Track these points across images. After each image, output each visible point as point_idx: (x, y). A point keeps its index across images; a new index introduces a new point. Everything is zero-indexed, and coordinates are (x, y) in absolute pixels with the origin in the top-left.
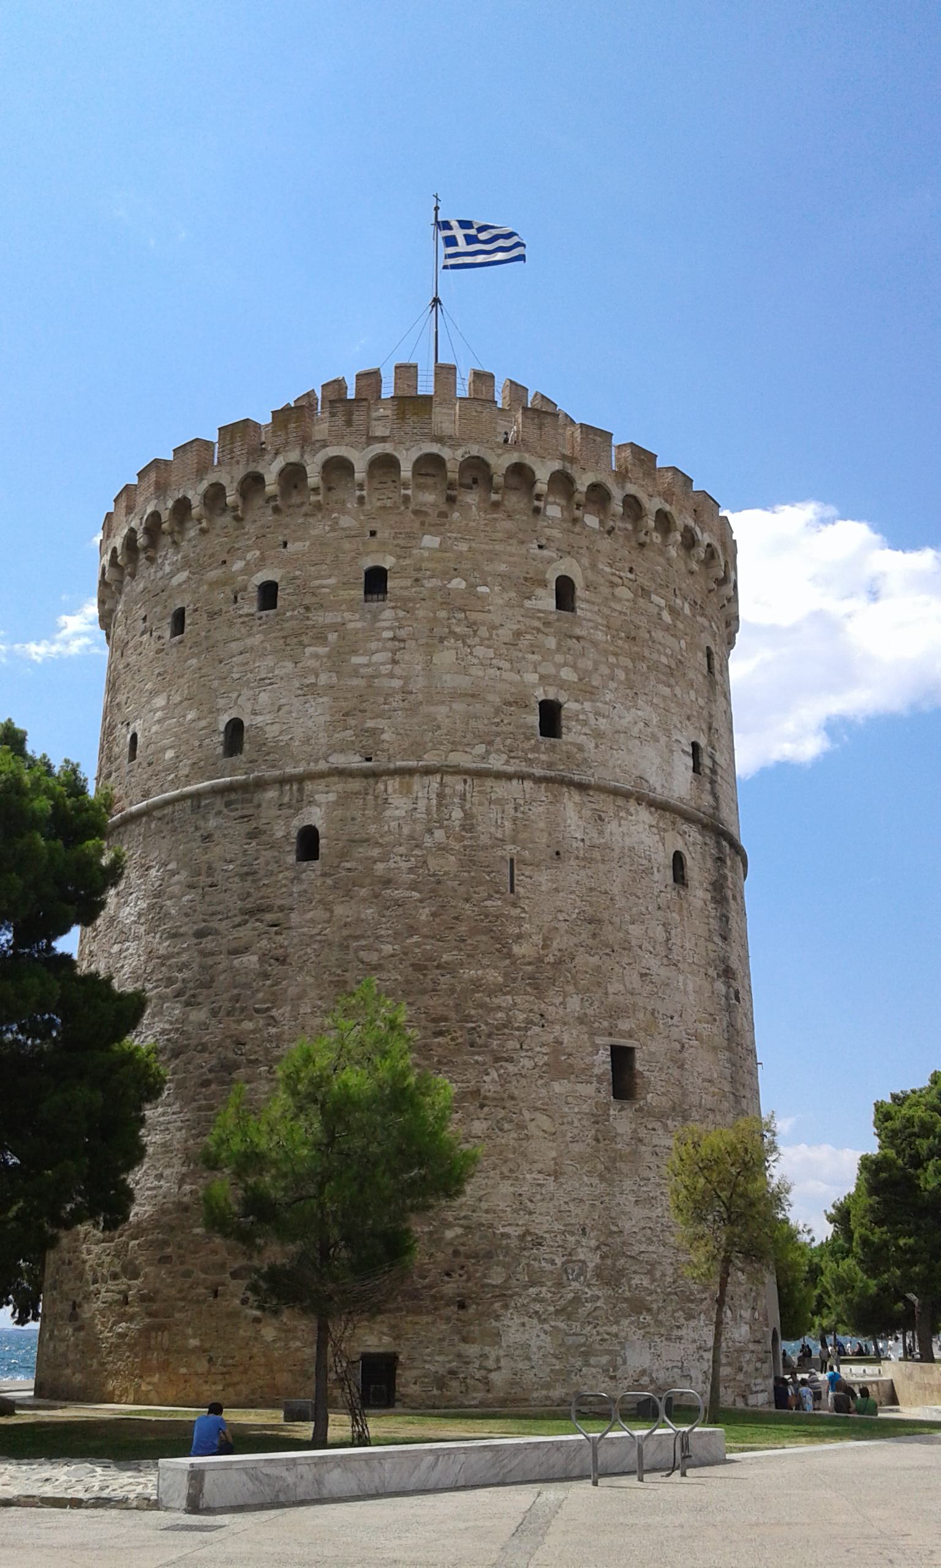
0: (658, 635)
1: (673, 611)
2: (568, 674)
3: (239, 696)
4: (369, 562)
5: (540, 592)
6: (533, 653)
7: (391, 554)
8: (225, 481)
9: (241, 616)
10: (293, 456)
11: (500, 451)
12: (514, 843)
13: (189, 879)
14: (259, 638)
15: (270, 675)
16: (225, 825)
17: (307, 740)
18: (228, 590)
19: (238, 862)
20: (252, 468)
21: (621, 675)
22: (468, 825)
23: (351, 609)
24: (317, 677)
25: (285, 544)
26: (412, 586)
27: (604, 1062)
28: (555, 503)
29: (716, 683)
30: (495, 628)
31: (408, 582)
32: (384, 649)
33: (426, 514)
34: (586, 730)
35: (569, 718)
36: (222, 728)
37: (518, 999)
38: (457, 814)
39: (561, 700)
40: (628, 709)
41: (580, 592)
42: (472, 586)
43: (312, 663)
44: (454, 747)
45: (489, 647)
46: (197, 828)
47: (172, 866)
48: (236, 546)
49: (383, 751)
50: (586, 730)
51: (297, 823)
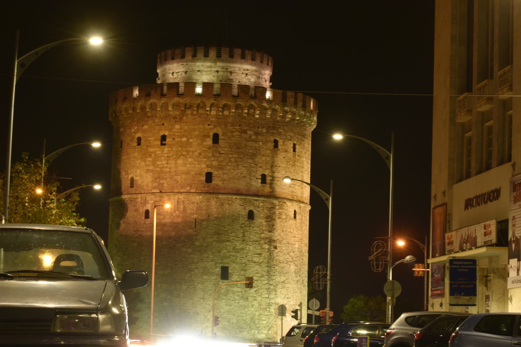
0: (250, 144)
1: (257, 134)
2: (215, 163)
4: (162, 134)
5: (208, 139)
6: (205, 158)
7: (168, 131)
11: (196, 98)
12: (196, 213)
17: (147, 186)
21: (233, 160)
22: (185, 210)
23: (157, 147)
24: (149, 166)
25: (143, 126)
26: (172, 141)
27: (219, 271)
28: (214, 110)
29: (279, 150)
30: (193, 152)
31: (171, 140)
32: (165, 160)
33: (176, 118)
34: (220, 179)
35: (214, 177)
36: (130, 179)
37: (196, 256)
38: (182, 207)
39: (212, 171)
40: (235, 171)
41: (220, 137)
42: (188, 140)
43: (148, 163)
44: (182, 187)
45: (192, 158)
49: (164, 189)
50: (220, 179)
51: (145, 208)
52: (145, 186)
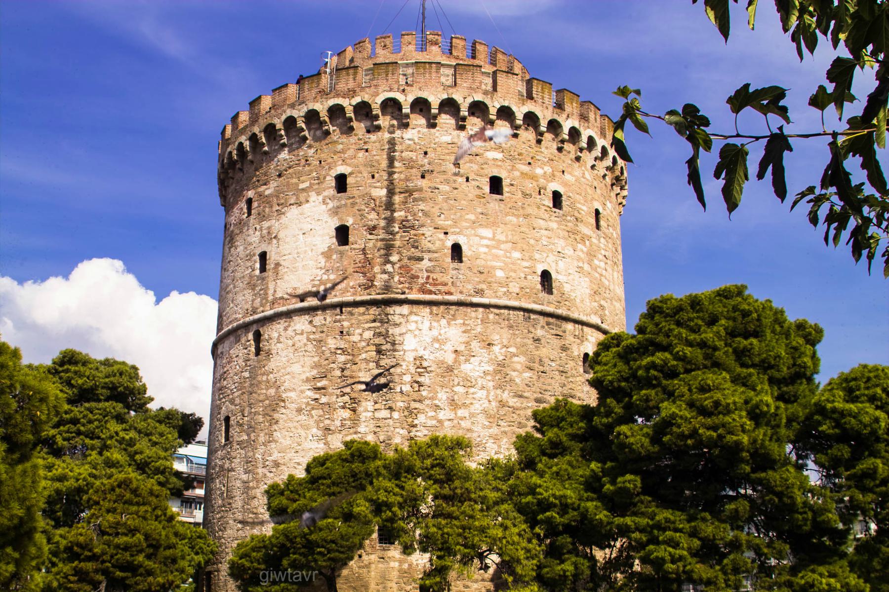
3: (547, 256)
8: (539, 114)
9: (544, 205)
10: (577, 125)
13: (527, 362)
14: (554, 225)
15: (563, 252)
16: (548, 336)
18: (535, 184)
19: (558, 363)
20: (556, 117)
36: (539, 273)
43: (582, 255)
46: (529, 332)
47: (513, 350)
48: (538, 157)
52: (578, 301)
